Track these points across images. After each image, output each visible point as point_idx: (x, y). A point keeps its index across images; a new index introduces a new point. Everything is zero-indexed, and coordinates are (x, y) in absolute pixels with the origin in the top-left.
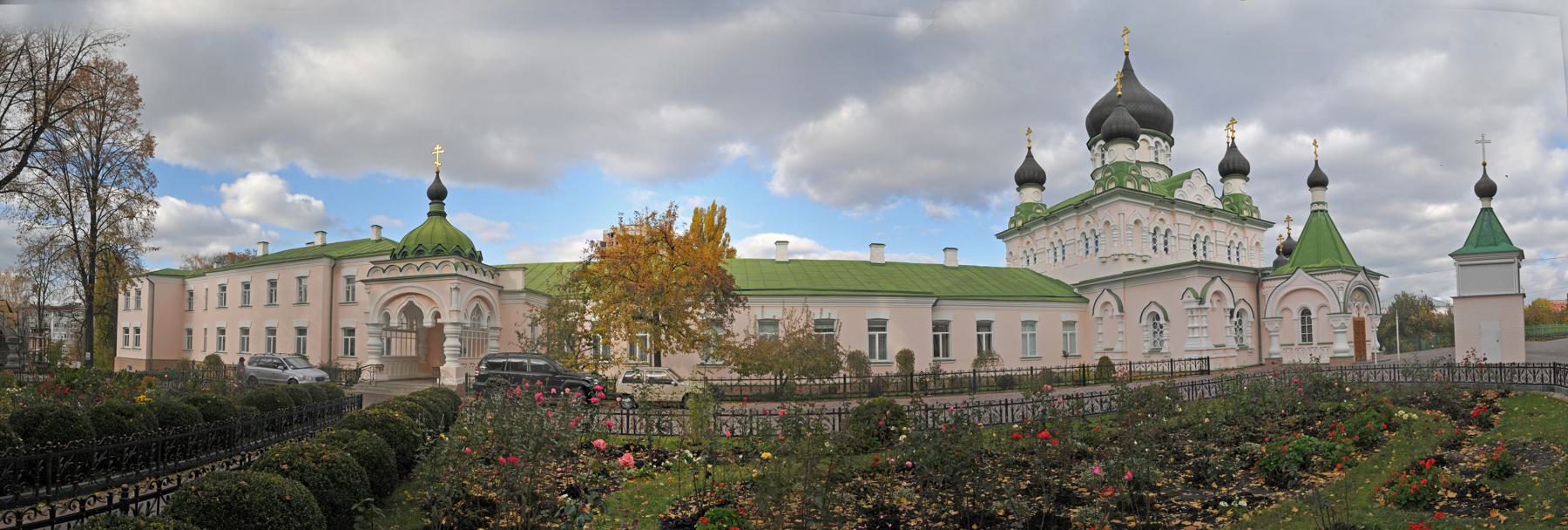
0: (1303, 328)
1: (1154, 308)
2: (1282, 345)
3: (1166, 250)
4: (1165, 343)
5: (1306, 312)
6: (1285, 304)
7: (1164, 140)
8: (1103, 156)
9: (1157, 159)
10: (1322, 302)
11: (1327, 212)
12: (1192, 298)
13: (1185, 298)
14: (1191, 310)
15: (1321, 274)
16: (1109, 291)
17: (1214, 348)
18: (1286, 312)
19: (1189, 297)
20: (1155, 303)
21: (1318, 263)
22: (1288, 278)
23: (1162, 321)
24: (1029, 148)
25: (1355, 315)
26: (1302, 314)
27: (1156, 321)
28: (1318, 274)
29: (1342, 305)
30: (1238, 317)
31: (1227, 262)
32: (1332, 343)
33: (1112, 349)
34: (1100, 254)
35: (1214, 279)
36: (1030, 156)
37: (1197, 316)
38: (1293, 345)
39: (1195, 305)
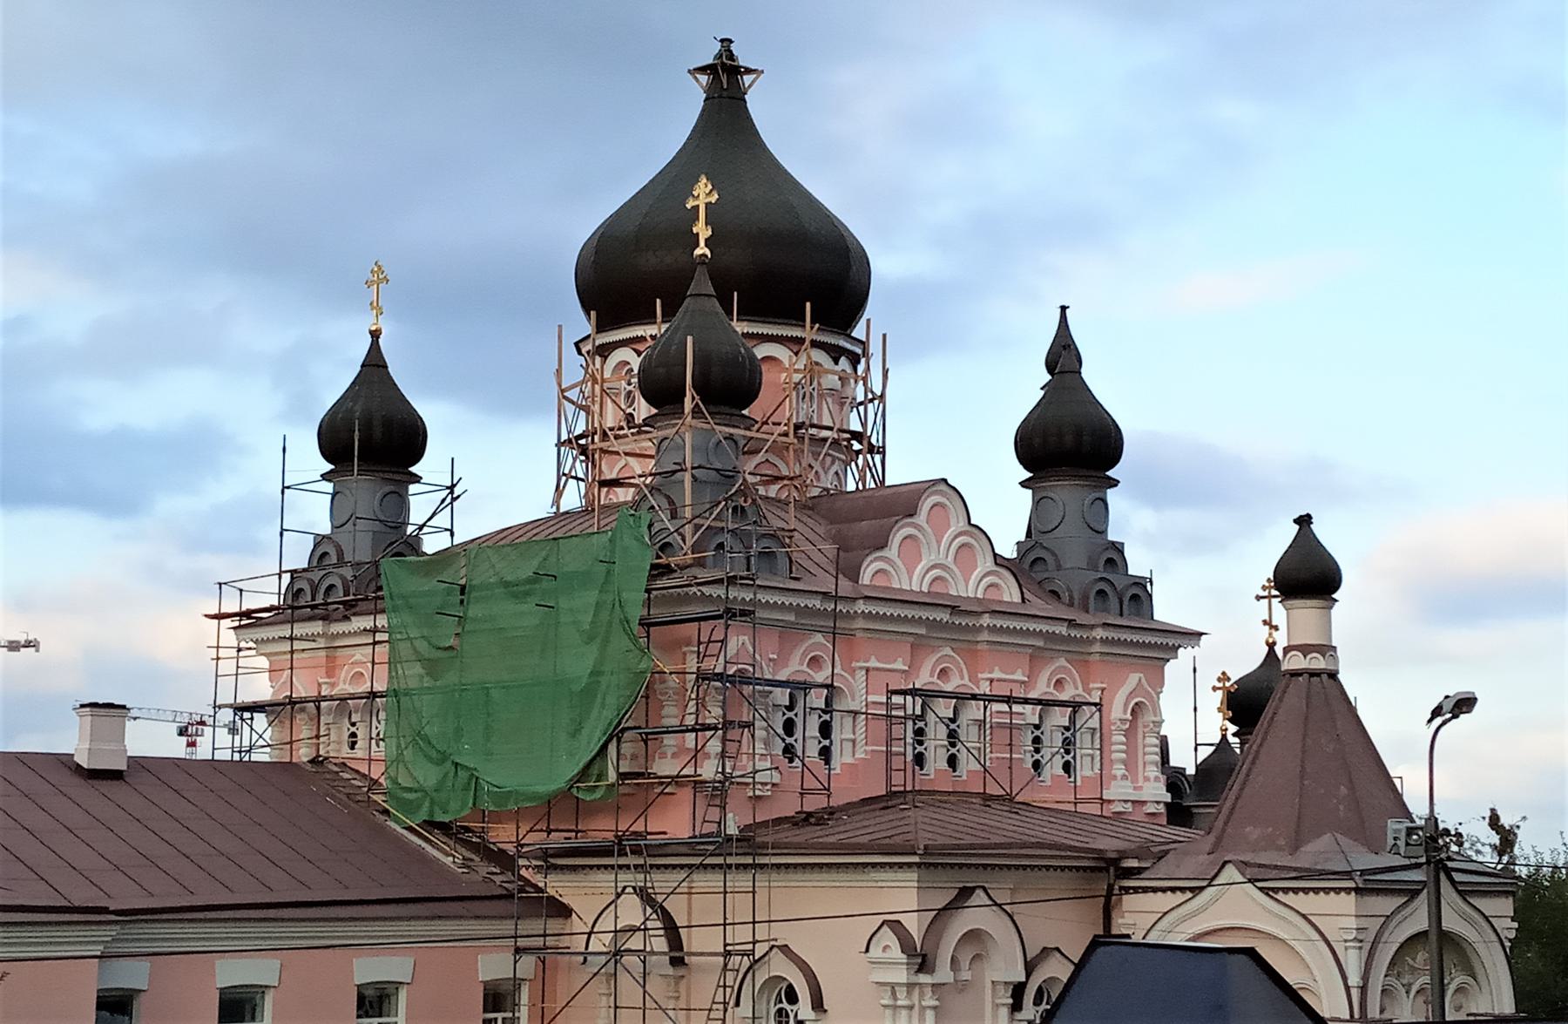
7: (836, 353)
11: (1333, 675)
12: (896, 953)
13: (876, 951)
14: (893, 987)
15: (1296, 891)
19: (886, 948)
22: (1196, 891)
24: (375, 335)
27: (785, 1005)
28: (1286, 890)
29: (1355, 993)
30: (1037, 1002)
35: (965, 893)
36: (374, 363)
39: (901, 976)
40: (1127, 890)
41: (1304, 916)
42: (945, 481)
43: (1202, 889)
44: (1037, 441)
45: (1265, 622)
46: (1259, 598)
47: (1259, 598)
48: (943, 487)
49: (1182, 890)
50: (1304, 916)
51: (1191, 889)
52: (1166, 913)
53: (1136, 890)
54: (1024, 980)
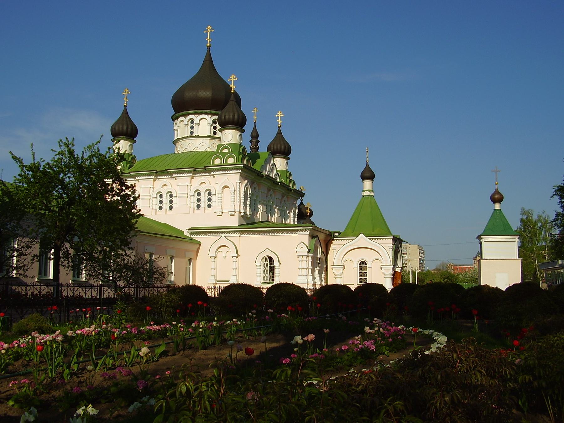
0: (361, 274)
5: (363, 263)
8: (192, 127)
10: (379, 257)
13: (298, 249)
20: (269, 249)
21: (373, 231)
26: (360, 264)
28: (375, 239)
36: (125, 113)
40: (334, 240)
43: (354, 239)
49: (349, 240)
51: (351, 239)
53: (337, 240)
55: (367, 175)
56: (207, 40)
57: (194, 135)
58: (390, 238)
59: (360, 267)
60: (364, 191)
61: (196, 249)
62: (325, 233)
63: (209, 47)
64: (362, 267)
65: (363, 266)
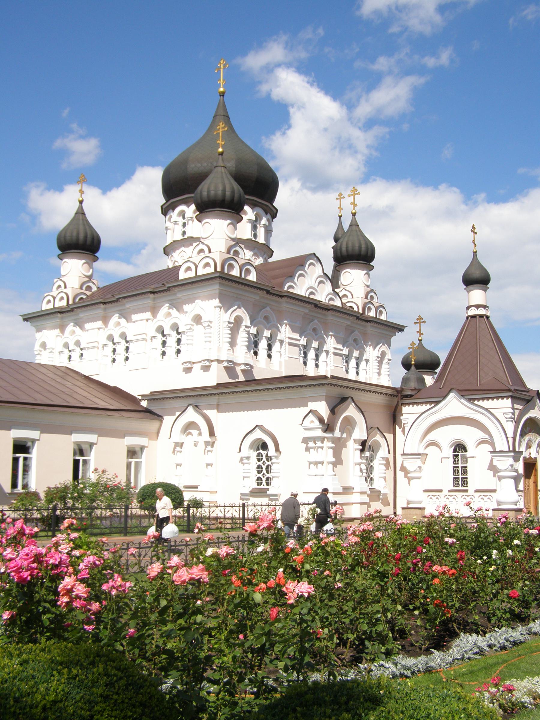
0: (455, 469)
1: (258, 434)
2: (425, 491)
3: (269, 356)
4: (273, 482)
6: (432, 436)
9: (255, 236)
12: (317, 423)
16: (196, 407)
17: (341, 490)
18: (432, 449)
23: (271, 451)
25: (526, 454)
26: (455, 451)
28: (478, 399)
29: (511, 440)
31: (343, 375)
32: (494, 491)
33: (196, 487)
34: (183, 357)
37: (322, 448)
38: (441, 491)
39: (319, 433)
41: (487, 410)
42: (314, 254)
44: (344, 249)
45: (418, 332)
46: (415, 323)
47: (415, 323)
48: (313, 256)
50: (487, 410)
52: (422, 413)
53: (409, 404)
54: (366, 438)
55: (476, 274)
56: (220, 83)
57: (186, 237)
58: (507, 397)
59: (454, 455)
60: (468, 308)
61: (156, 431)
62: (384, 394)
63: (222, 94)
64: (458, 455)
65: (460, 454)
